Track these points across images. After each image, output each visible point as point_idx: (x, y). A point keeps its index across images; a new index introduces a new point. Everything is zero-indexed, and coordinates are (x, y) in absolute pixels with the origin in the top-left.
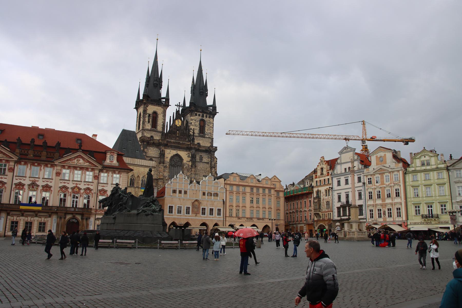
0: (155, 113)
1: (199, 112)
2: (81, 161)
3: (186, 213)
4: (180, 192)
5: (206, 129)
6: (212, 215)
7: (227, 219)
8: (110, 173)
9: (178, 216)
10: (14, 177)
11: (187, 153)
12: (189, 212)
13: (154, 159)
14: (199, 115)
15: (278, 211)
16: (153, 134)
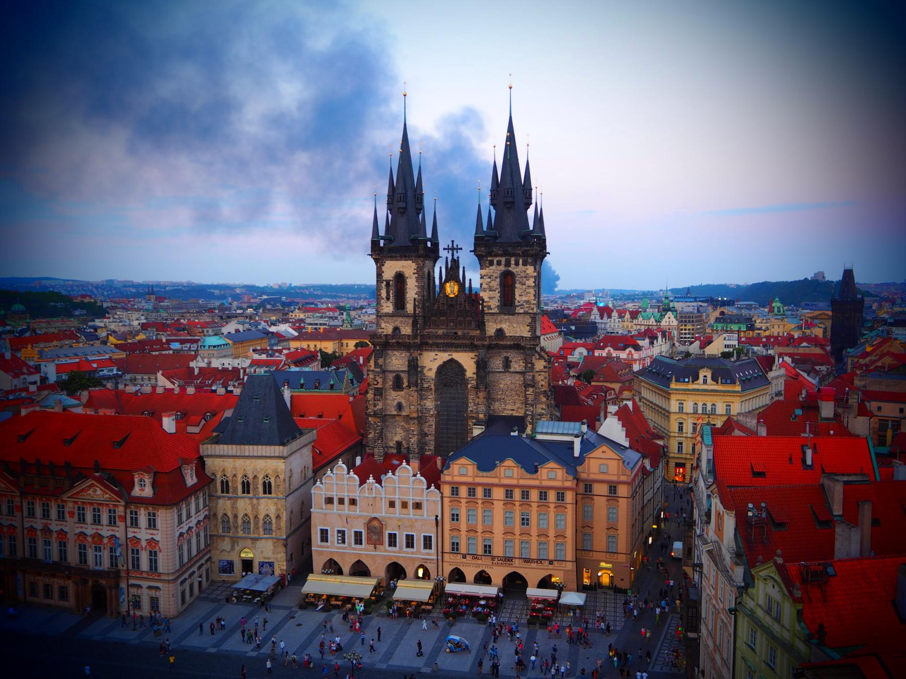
1: (496, 256)
2: (99, 492)
3: (356, 543)
4: (341, 501)
5: (517, 292)
6: (413, 547)
7: (446, 556)
8: (142, 509)
9: (338, 548)
10: (25, 519)
11: (472, 355)
12: (361, 540)
13: (403, 375)
14: (499, 263)
15: (612, 532)
16: (398, 322)
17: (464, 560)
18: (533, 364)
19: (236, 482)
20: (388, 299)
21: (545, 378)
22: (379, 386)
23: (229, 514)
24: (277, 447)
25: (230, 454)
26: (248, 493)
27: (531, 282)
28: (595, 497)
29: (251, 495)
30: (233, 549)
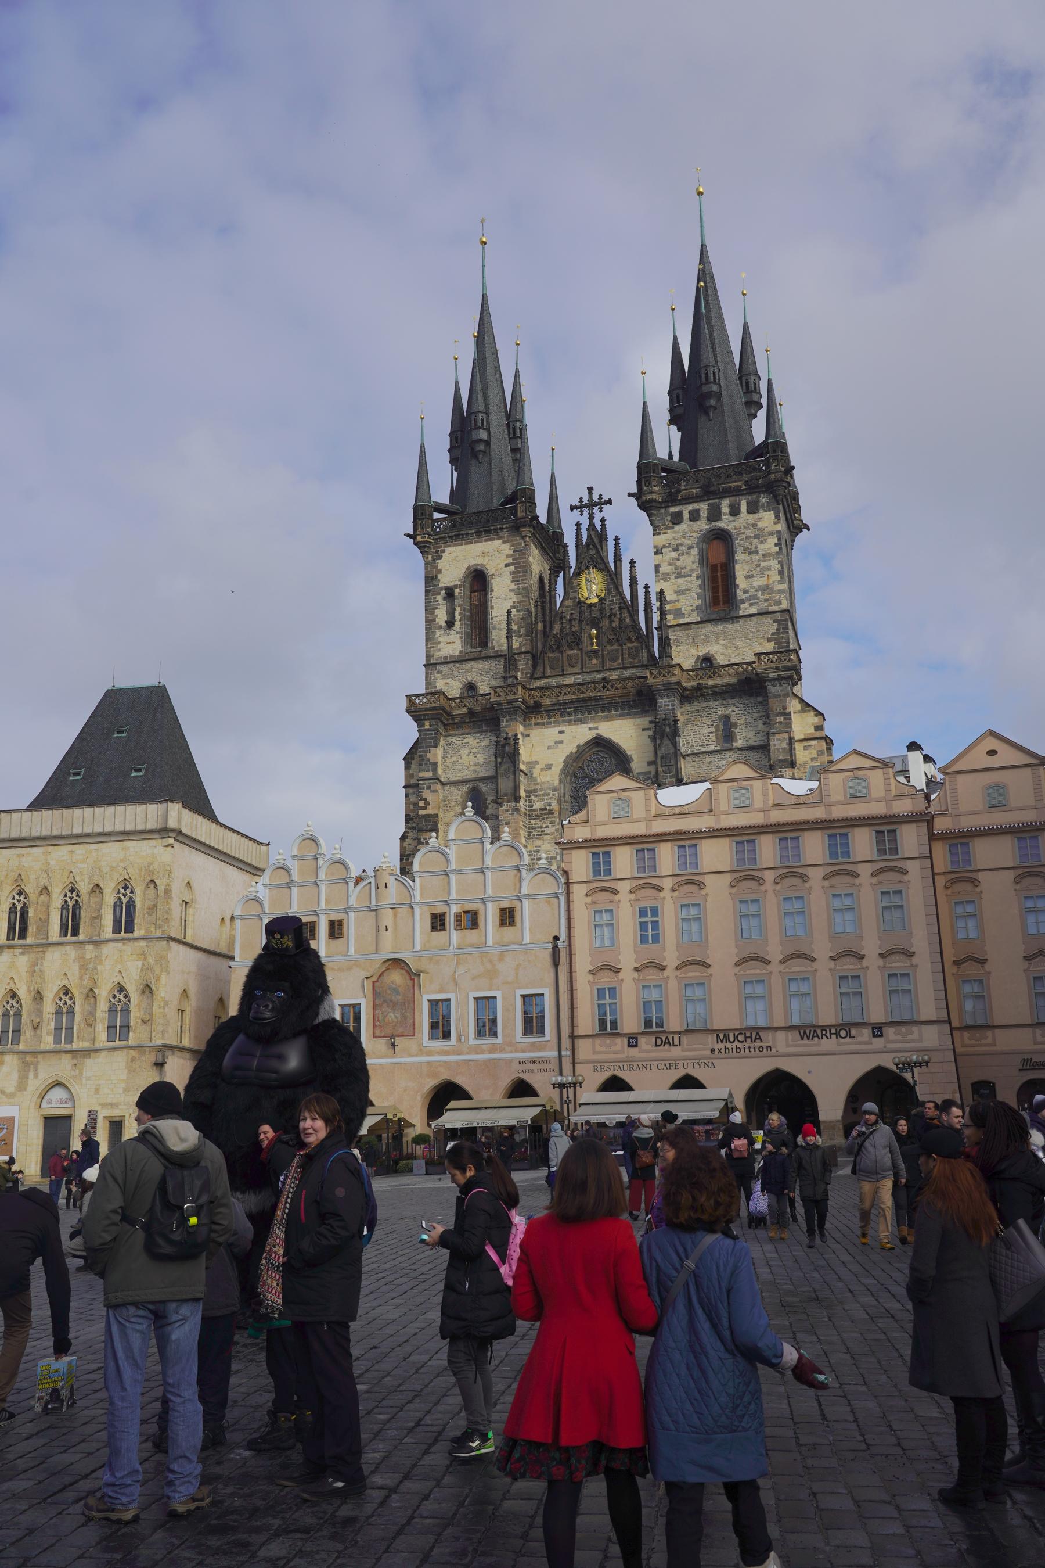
0: (478, 579)
1: (687, 500)
5: (740, 572)
7: (584, 1048)
11: (644, 721)
13: (484, 787)
14: (694, 516)
17: (633, 1051)
18: (787, 715)
19: (48, 905)
20: (450, 624)
21: (820, 753)
22: (429, 811)
23: (22, 993)
24: (152, 808)
25: (35, 833)
26: (75, 932)
27: (770, 545)
28: (981, 876)
29: (81, 937)
30: (22, 1086)
